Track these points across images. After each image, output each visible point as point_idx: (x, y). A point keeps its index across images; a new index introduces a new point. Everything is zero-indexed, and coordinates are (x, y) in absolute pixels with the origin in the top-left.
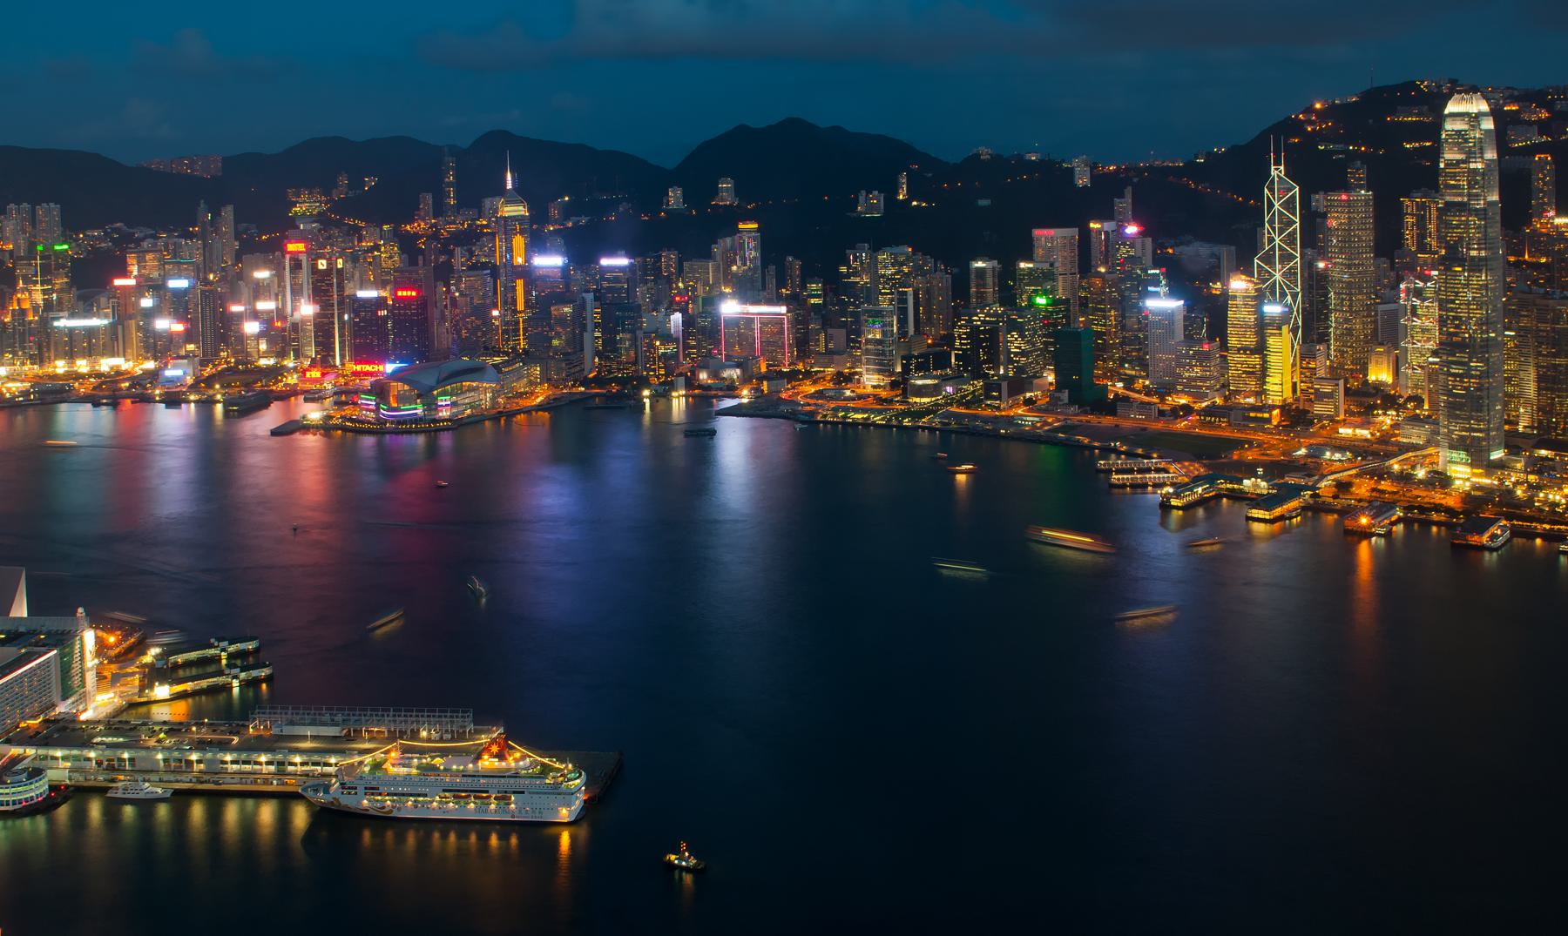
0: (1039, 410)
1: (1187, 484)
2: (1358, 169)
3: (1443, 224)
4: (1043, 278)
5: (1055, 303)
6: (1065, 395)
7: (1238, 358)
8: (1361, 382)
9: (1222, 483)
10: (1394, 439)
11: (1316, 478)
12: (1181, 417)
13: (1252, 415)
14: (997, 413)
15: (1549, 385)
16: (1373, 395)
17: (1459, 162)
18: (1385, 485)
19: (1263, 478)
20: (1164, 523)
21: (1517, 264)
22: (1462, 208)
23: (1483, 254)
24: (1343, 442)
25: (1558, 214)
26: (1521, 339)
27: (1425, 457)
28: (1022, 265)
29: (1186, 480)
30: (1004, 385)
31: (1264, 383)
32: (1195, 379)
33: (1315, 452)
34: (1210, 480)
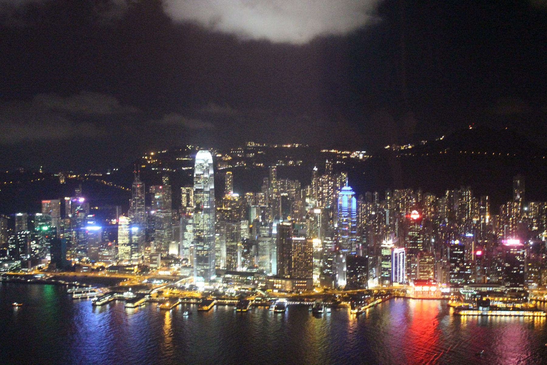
0: (44, 271)
1: (102, 296)
2: (166, 177)
3: (196, 197)
4: (46, 220)
5: (51, 229)
6: (55, 265)
7: (123, 247)
8: (167, 254)
9: (115, 295)
10: (178, 274)
11: (150, 290)
12: (101, 270)
13: (127, 268)
14: (27, 274)
15: (230, 252)
16: (171, 259)
17: (200, 175)
18: (175, 291)
19: (131, 291)
20: (94, 311)
21: (220, 210)
22: (201, 191)
23: (209, 207)
24: (160, 277)
25: (234, 192)
26: (221, 237)
27: (189, 280)
28: (38, 214)
29: (102, 294)
30: (30, 262)
31: (132, 257)
32: (106, 256)
33: (151, 280)
34: (111, 294)
